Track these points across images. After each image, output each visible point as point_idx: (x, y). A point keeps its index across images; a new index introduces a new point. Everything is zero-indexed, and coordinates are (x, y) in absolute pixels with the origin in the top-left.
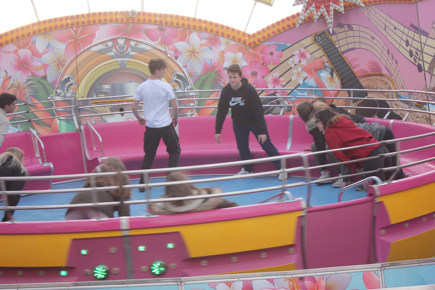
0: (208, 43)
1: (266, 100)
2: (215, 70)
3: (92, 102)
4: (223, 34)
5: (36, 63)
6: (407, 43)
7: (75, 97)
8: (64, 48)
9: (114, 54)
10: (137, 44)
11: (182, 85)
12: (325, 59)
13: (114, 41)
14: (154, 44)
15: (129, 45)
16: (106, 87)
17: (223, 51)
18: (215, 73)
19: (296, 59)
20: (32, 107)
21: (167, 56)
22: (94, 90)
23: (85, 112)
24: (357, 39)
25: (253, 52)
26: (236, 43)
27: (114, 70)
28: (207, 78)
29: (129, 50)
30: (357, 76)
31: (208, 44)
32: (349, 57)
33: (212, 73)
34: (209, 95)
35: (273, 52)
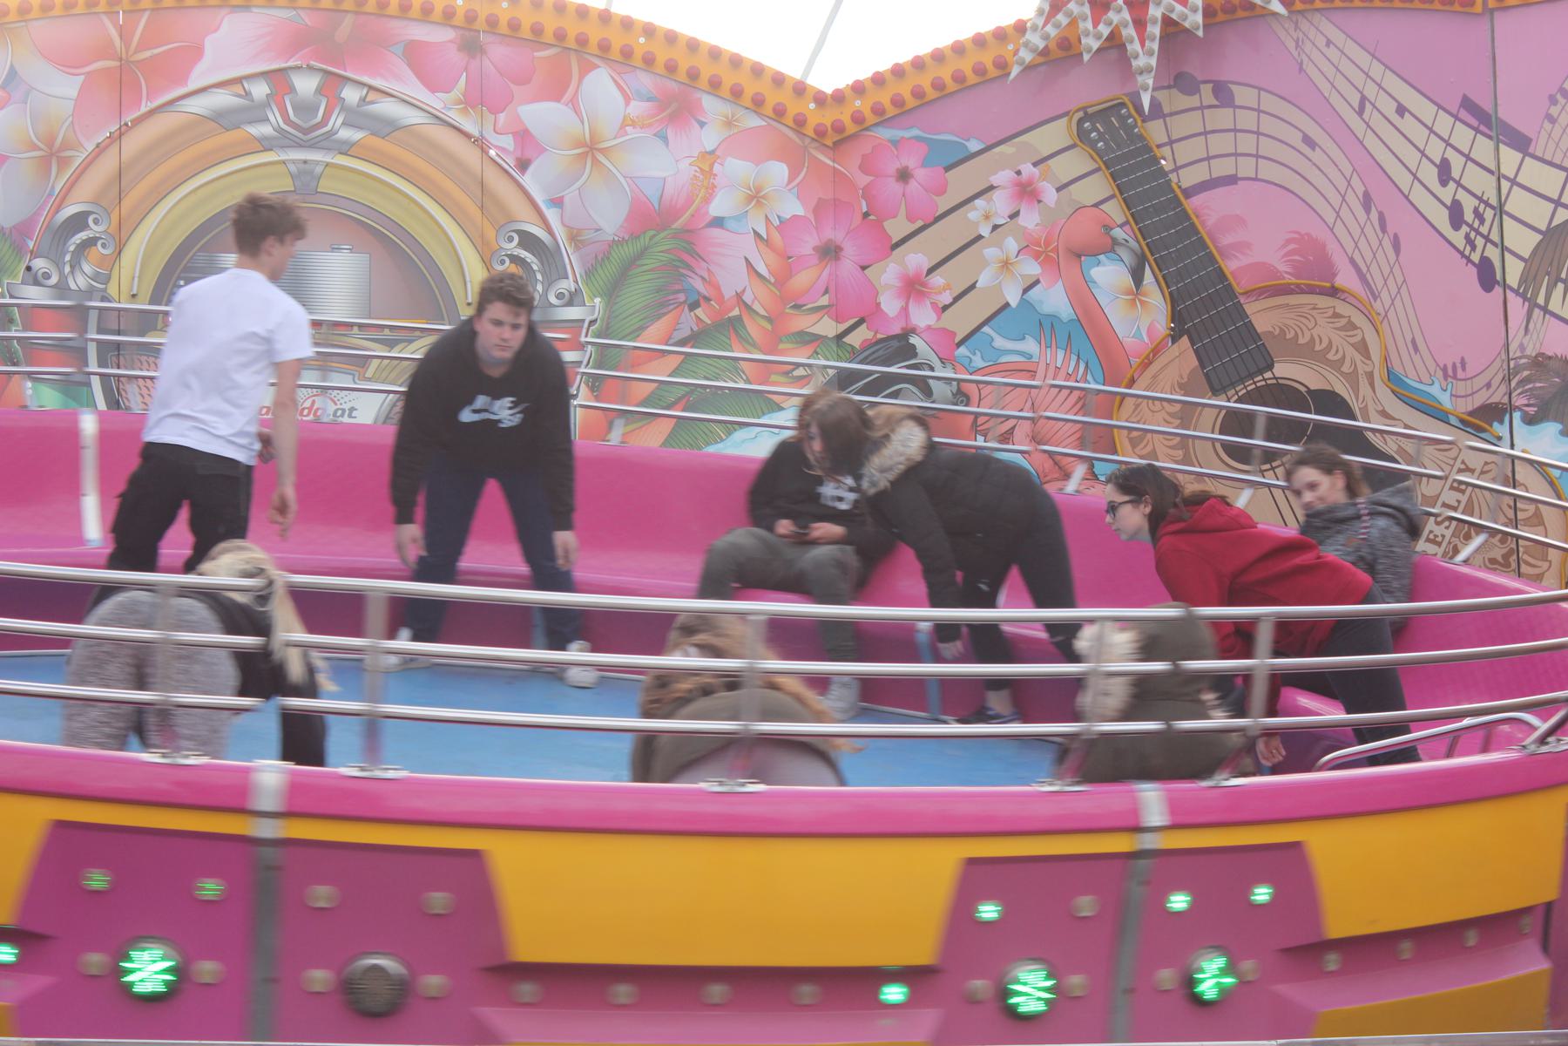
2: (674, 227)
4: (715, 84)
7: (105, 294)
8: (74, 94)
9: (276, 131)
10: (367, 100)
11: (539, 277)
12: (1115, 211)
13: (279, 79)
14: (435, 101)
15: (335, 101)
17: (713, 152)
18: (675, 236)
19: (1000, 204)
21: (487, 153)
22: (180, 273)
23: (141, 355)
24: (1247, 143)
25: (831, 163)
26: (764, 123)
28: (641, 254)
30: (1238, 290)
31: (651, 121)
32: (1210, 210)
33: (662, 235)
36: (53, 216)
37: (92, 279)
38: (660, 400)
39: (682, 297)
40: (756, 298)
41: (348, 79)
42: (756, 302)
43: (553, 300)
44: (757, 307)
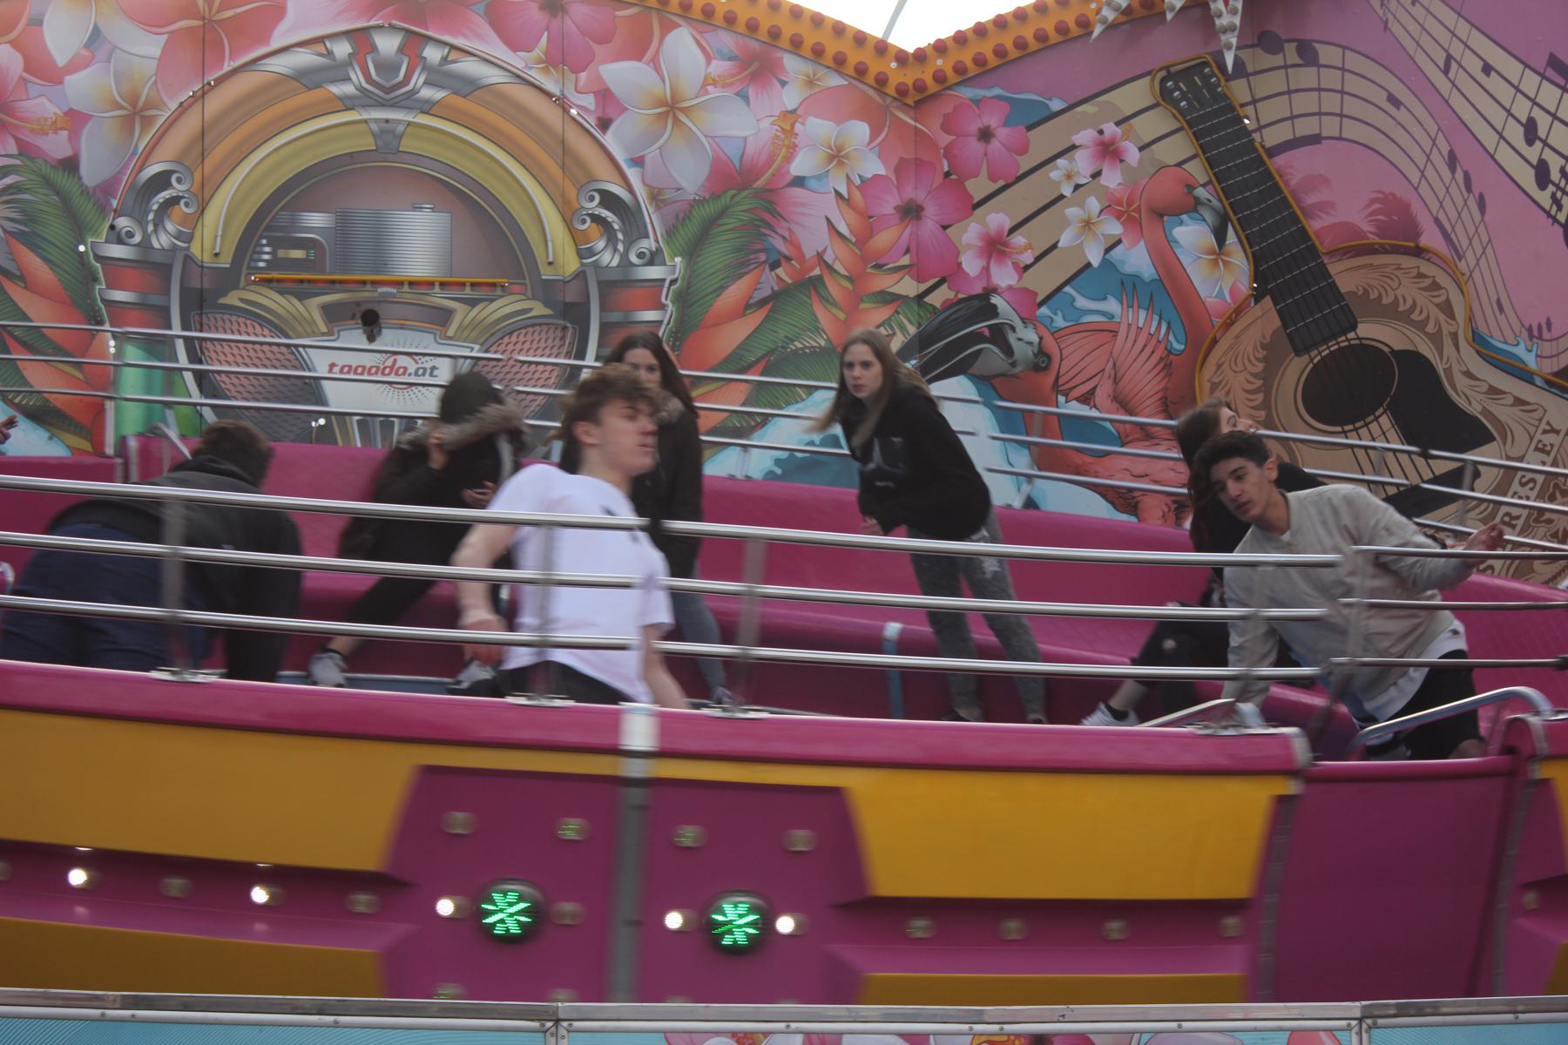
0: (734, 75)
1: (954, 317)
2: (755, 186)
3: (253, 278)
4: (796, 44)
5: (41, 105)
6: (1530, 129)
7: (187, 252)
8: (158, 53)
9: (357, 89)
10: (449, 59)
11: (620, 236)
12: (1198, 171)
13: (360, 38)
14: (517, 61)
15: (417, 60)
16: (316, 220)
17: (794, 112)
19: (1083, 163)
20: (10, 280)
21: (568, 112)
22: (265, 230)
23: (223, 313)
24: (1331, 102)
25: (912, 123)
26: (846, 83)
27: (351, 154)
28: (723, 213)
29: (418, 79)
30: (1321, 249)
32: (1294, 168)
33: (743, 194)
34: (726, 280)
35: (992, 127)
36: (137, 175)
37: (173, 237)
38: (741, 359)
39: (763, 257)
40: (837, 258)
41: (430, 38)
42: (837, 262)
43: (634, 259)
44: (838, 267)
